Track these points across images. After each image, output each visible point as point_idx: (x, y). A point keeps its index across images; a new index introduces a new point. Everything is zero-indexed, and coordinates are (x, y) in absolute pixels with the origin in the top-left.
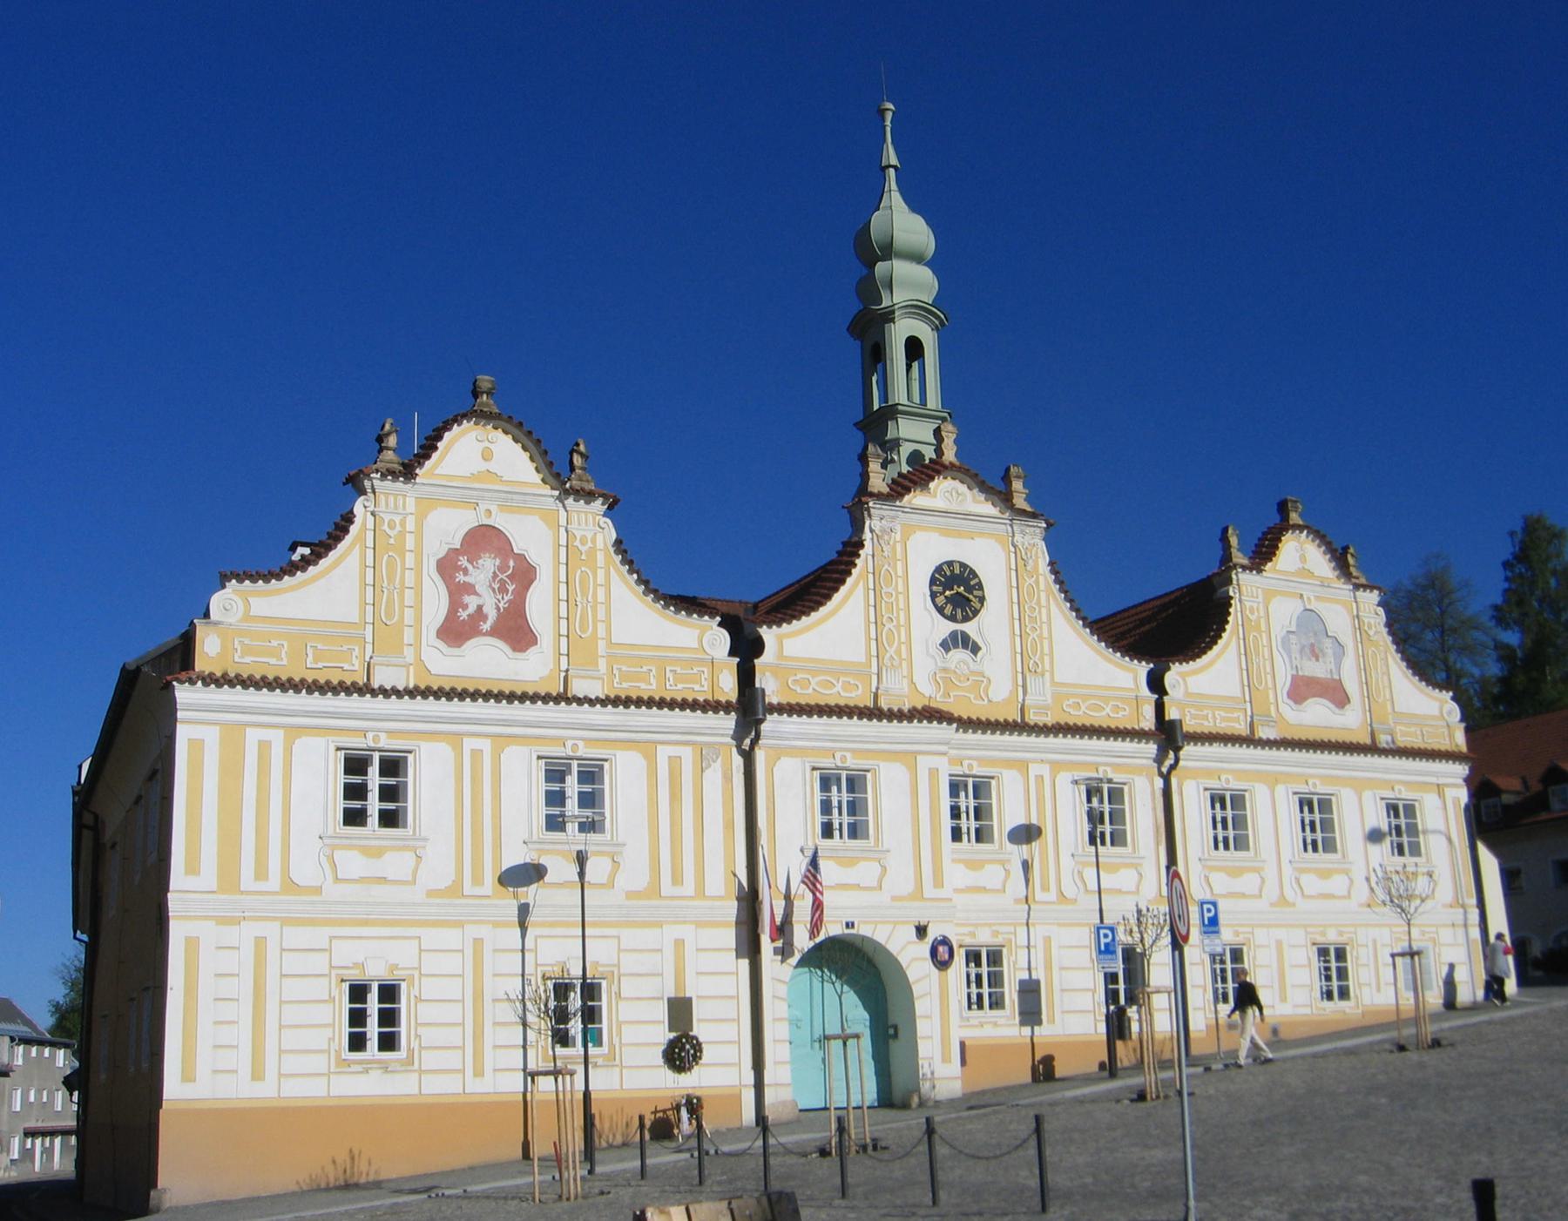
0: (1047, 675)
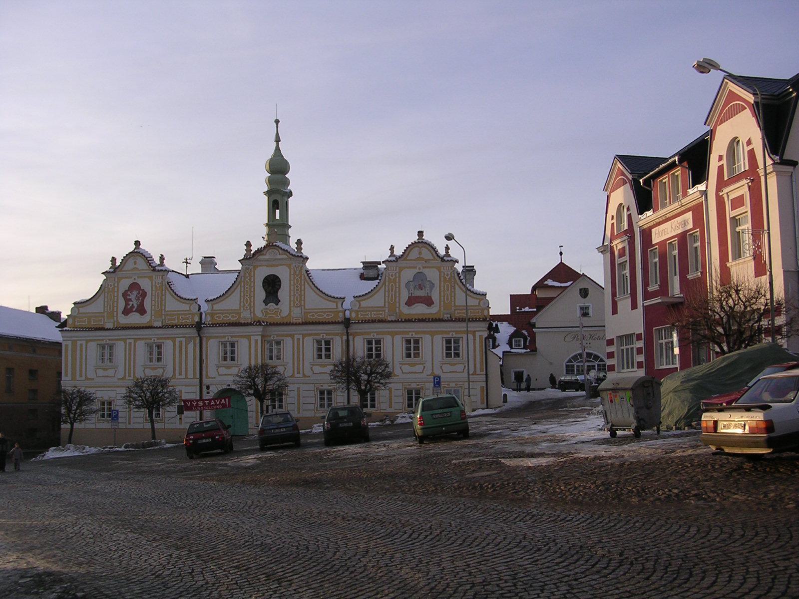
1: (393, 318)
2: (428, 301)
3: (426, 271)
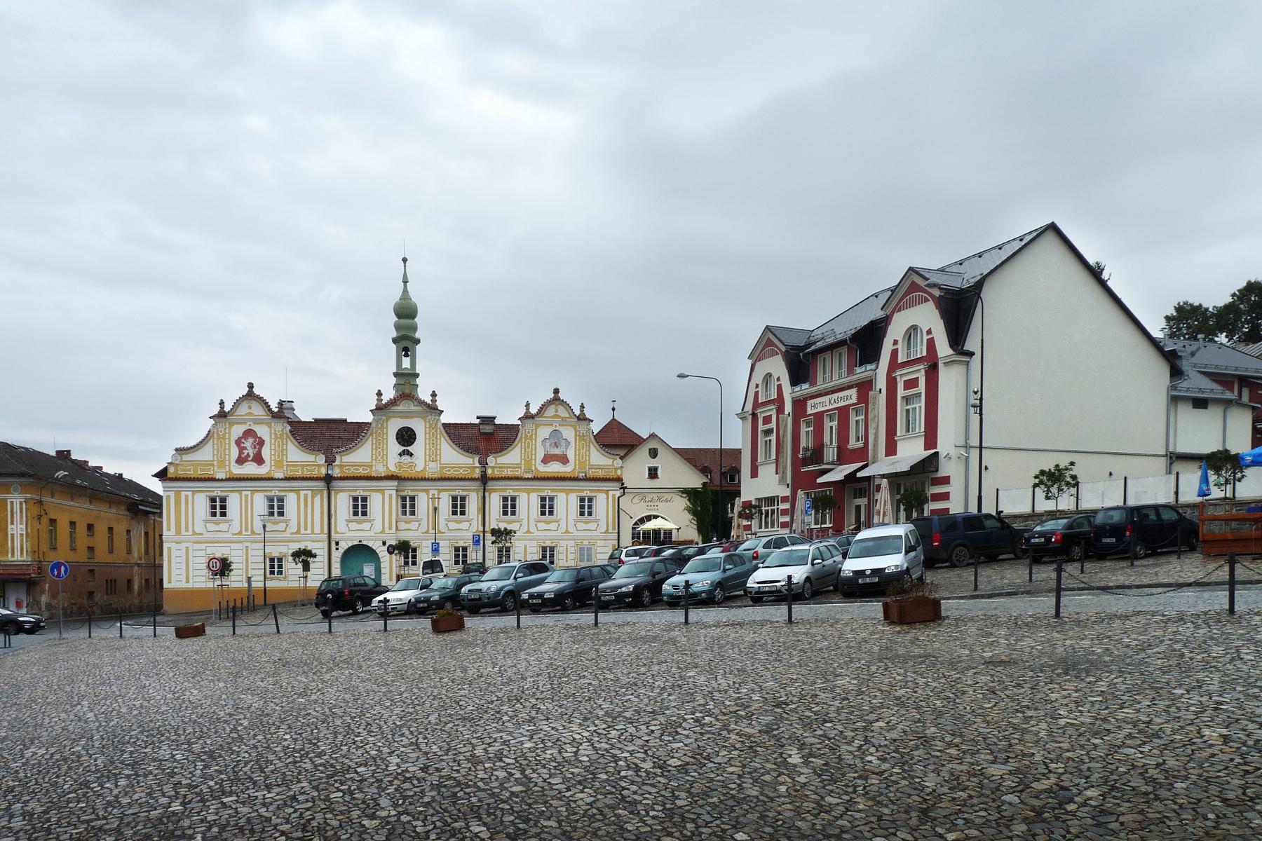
2: (564, 460)
3: (562, 429)
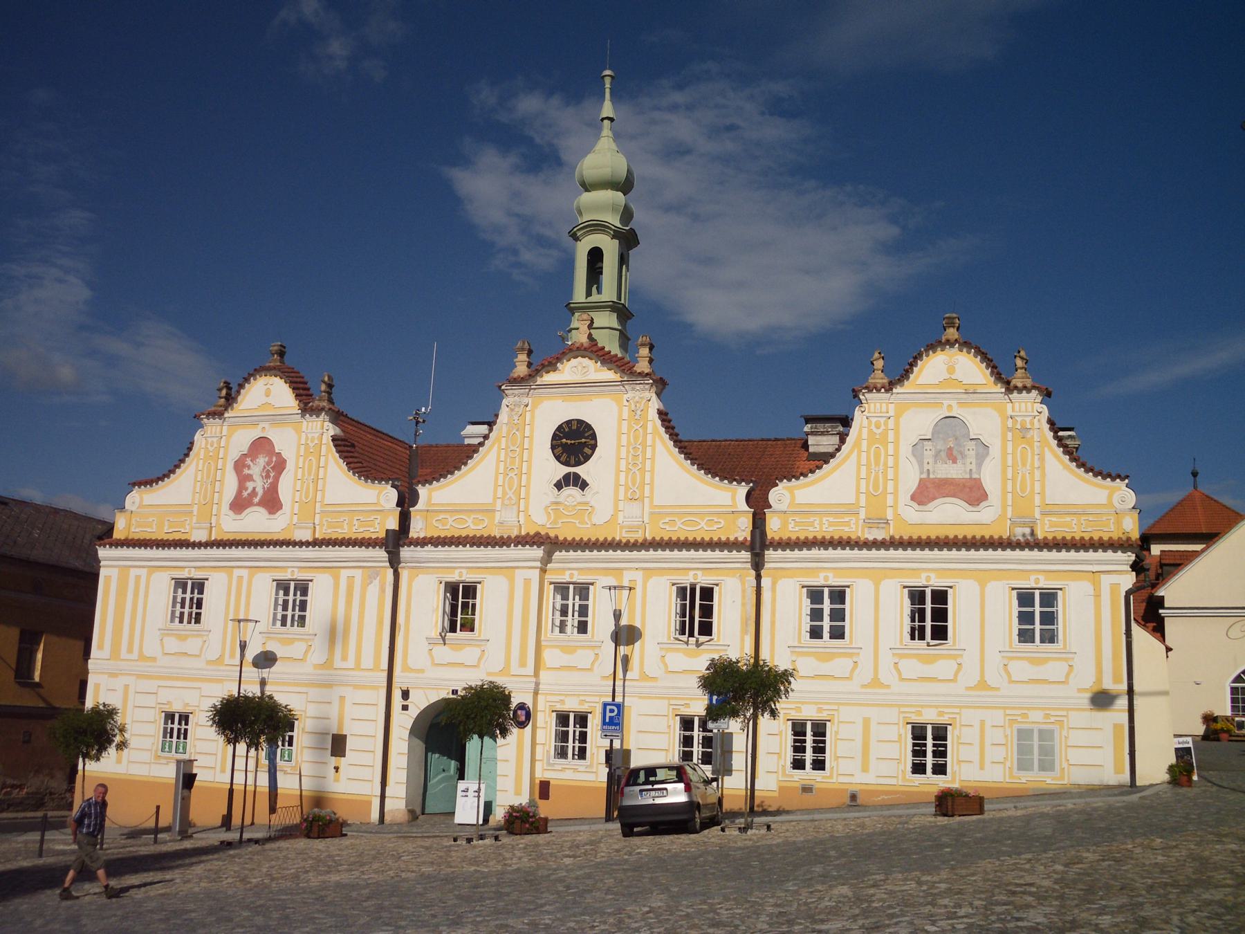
0: (646, 500)
1: (879, 535)
2: (973, 493)
